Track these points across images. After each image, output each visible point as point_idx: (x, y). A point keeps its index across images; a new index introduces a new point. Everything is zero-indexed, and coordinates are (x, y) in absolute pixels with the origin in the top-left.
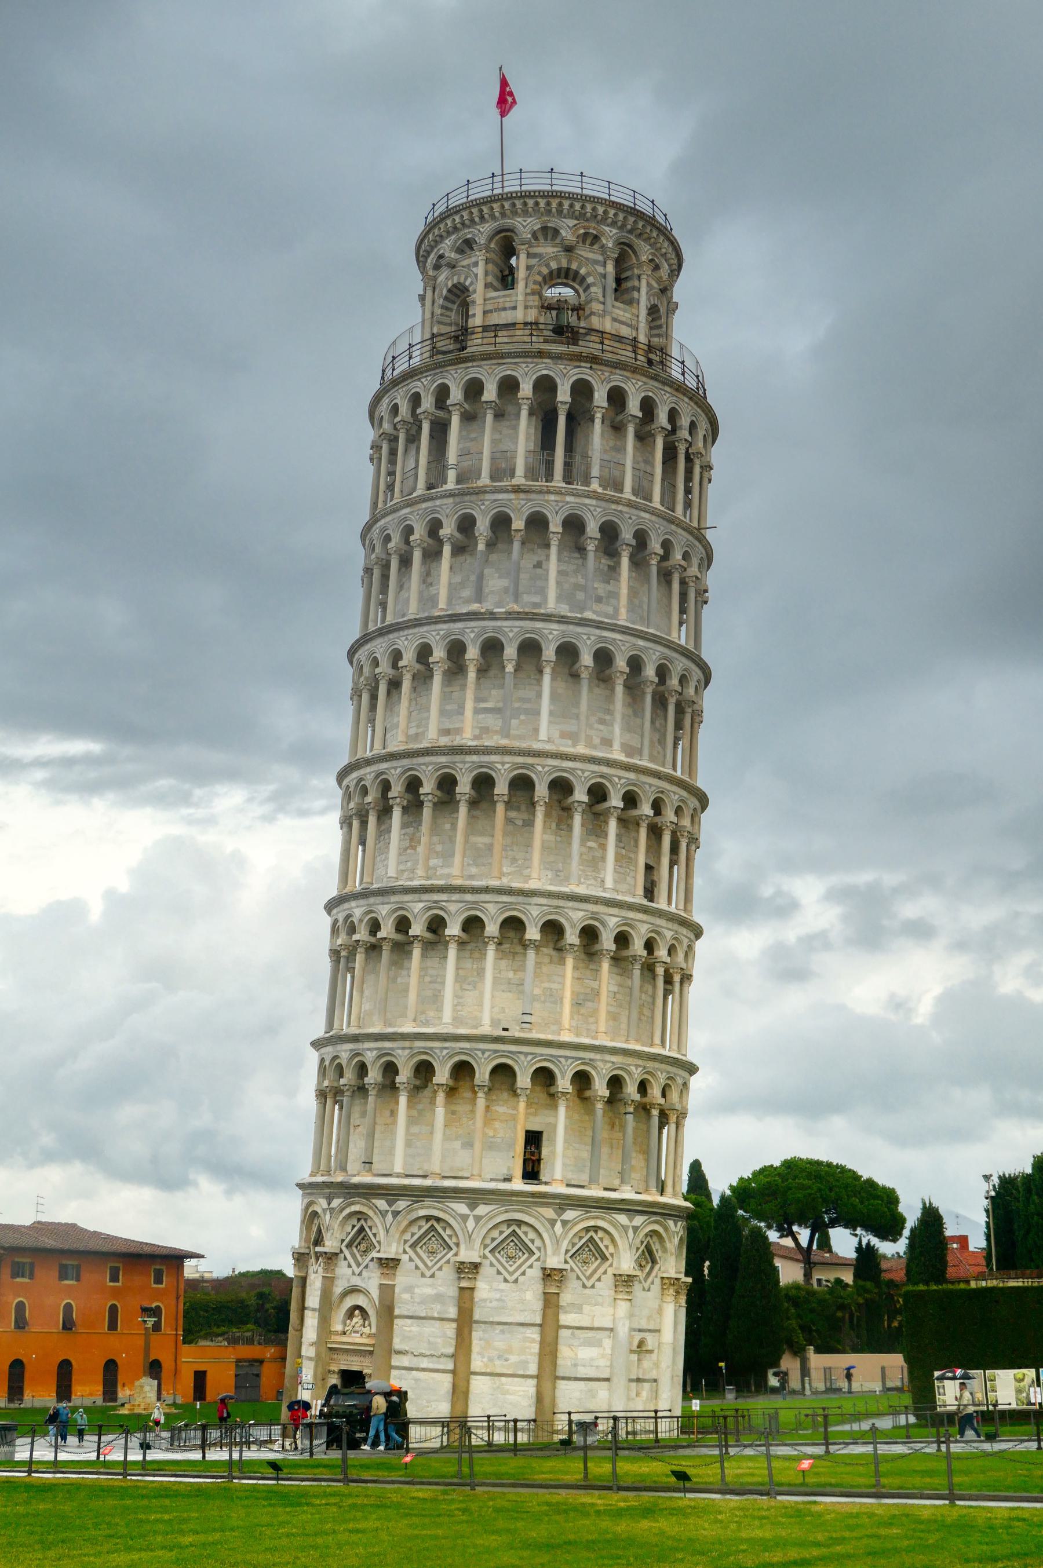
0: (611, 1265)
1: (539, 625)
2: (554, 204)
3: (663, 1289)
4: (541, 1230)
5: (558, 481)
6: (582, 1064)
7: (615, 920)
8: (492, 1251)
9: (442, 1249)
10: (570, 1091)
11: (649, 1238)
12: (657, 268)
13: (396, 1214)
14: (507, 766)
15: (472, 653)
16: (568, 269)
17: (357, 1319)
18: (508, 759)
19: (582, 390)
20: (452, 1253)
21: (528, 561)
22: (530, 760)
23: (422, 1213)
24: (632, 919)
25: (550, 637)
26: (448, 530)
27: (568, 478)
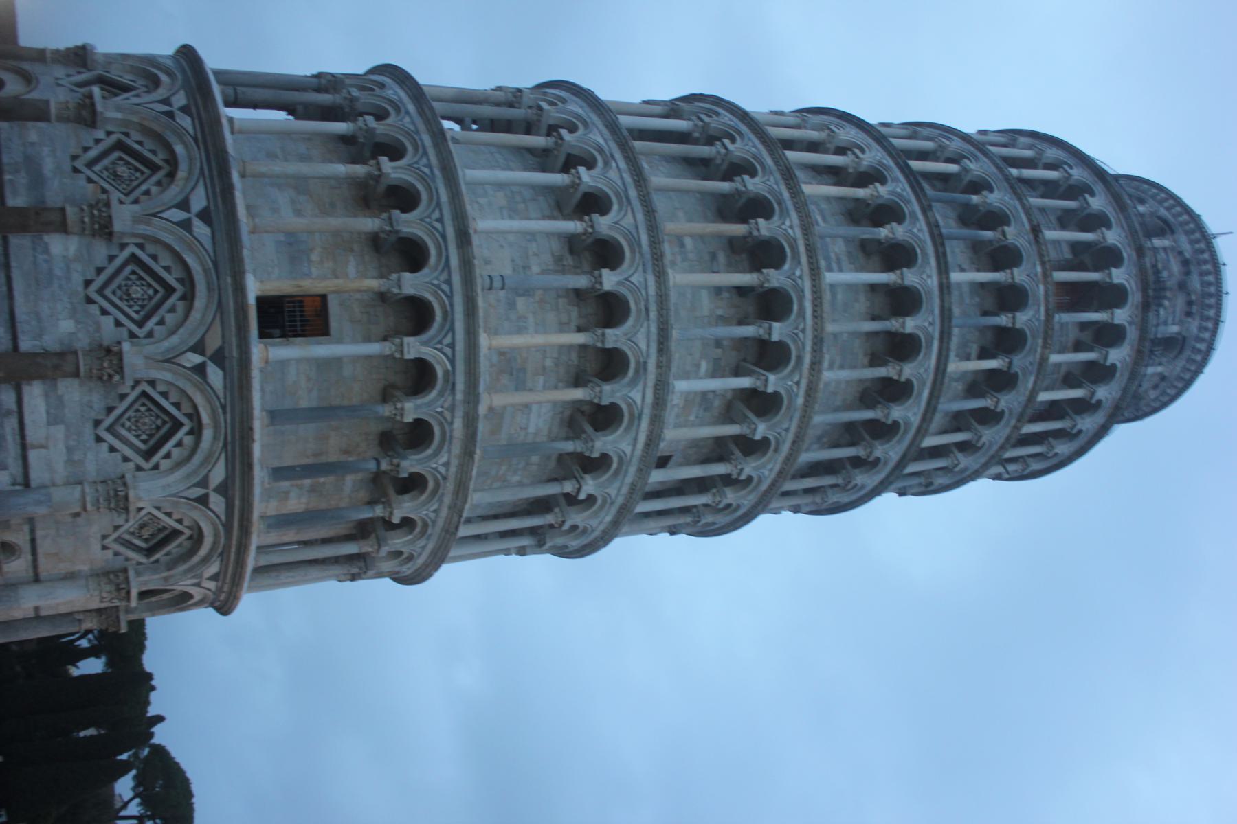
0: (139, 468)
1: (933, 261)
2: (1208, 267)
3: (106, 573)
6: (446, 373)
8: (134, 258)
9: (125, 186)
10: (407, 357)
11: (187, 532)
14: (790, 231)
16: (1164, 289)
18: (798, 233)
20: (122, 196)
22: (804, 259)
23: (179, 149)
24: (639, 425)
25: (924, 276)
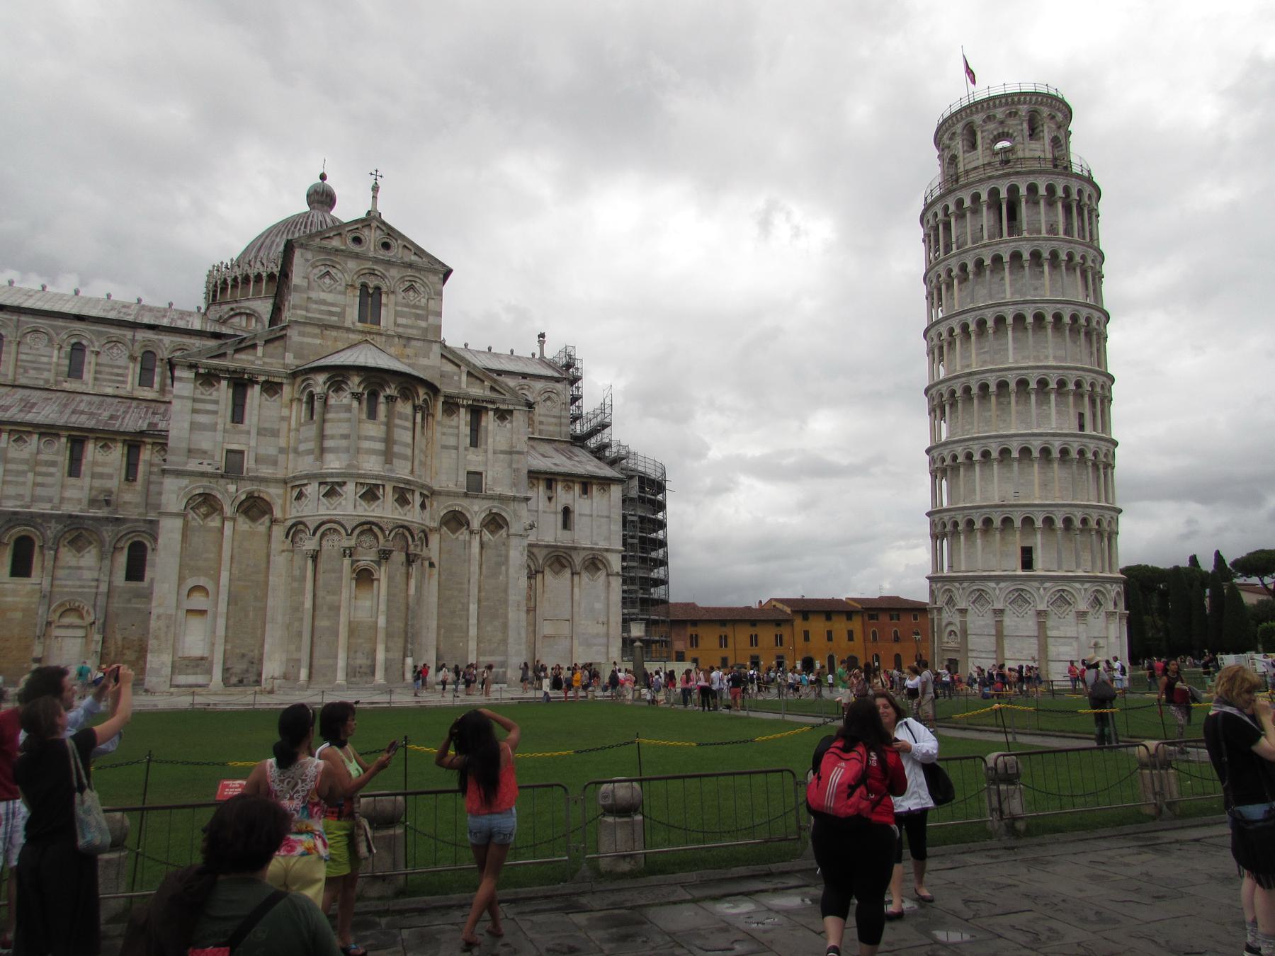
1: (1003, 308)
4: (1033, 592)
5: (1005, 237)
7: (1058, 443)
8: (1010, 603)
12: (1053, 117)
13: (963, 589)
15: (972, 327)
17: (953, 636)
18: (994, 374)
19: (1013, 190)
21: (996, 279)
22: (1004, 373)
23: (975, 588)
26: (955, 272)
27: (1010, 234)
